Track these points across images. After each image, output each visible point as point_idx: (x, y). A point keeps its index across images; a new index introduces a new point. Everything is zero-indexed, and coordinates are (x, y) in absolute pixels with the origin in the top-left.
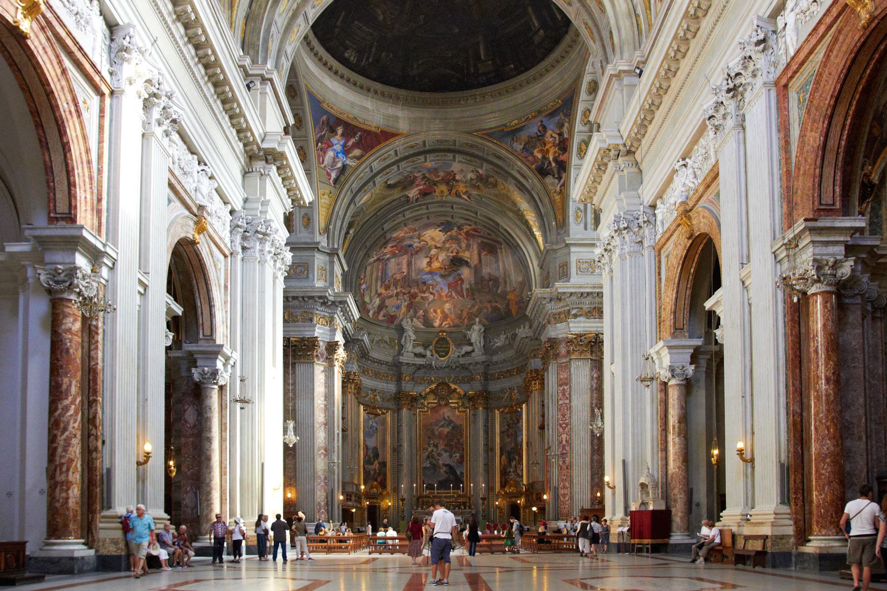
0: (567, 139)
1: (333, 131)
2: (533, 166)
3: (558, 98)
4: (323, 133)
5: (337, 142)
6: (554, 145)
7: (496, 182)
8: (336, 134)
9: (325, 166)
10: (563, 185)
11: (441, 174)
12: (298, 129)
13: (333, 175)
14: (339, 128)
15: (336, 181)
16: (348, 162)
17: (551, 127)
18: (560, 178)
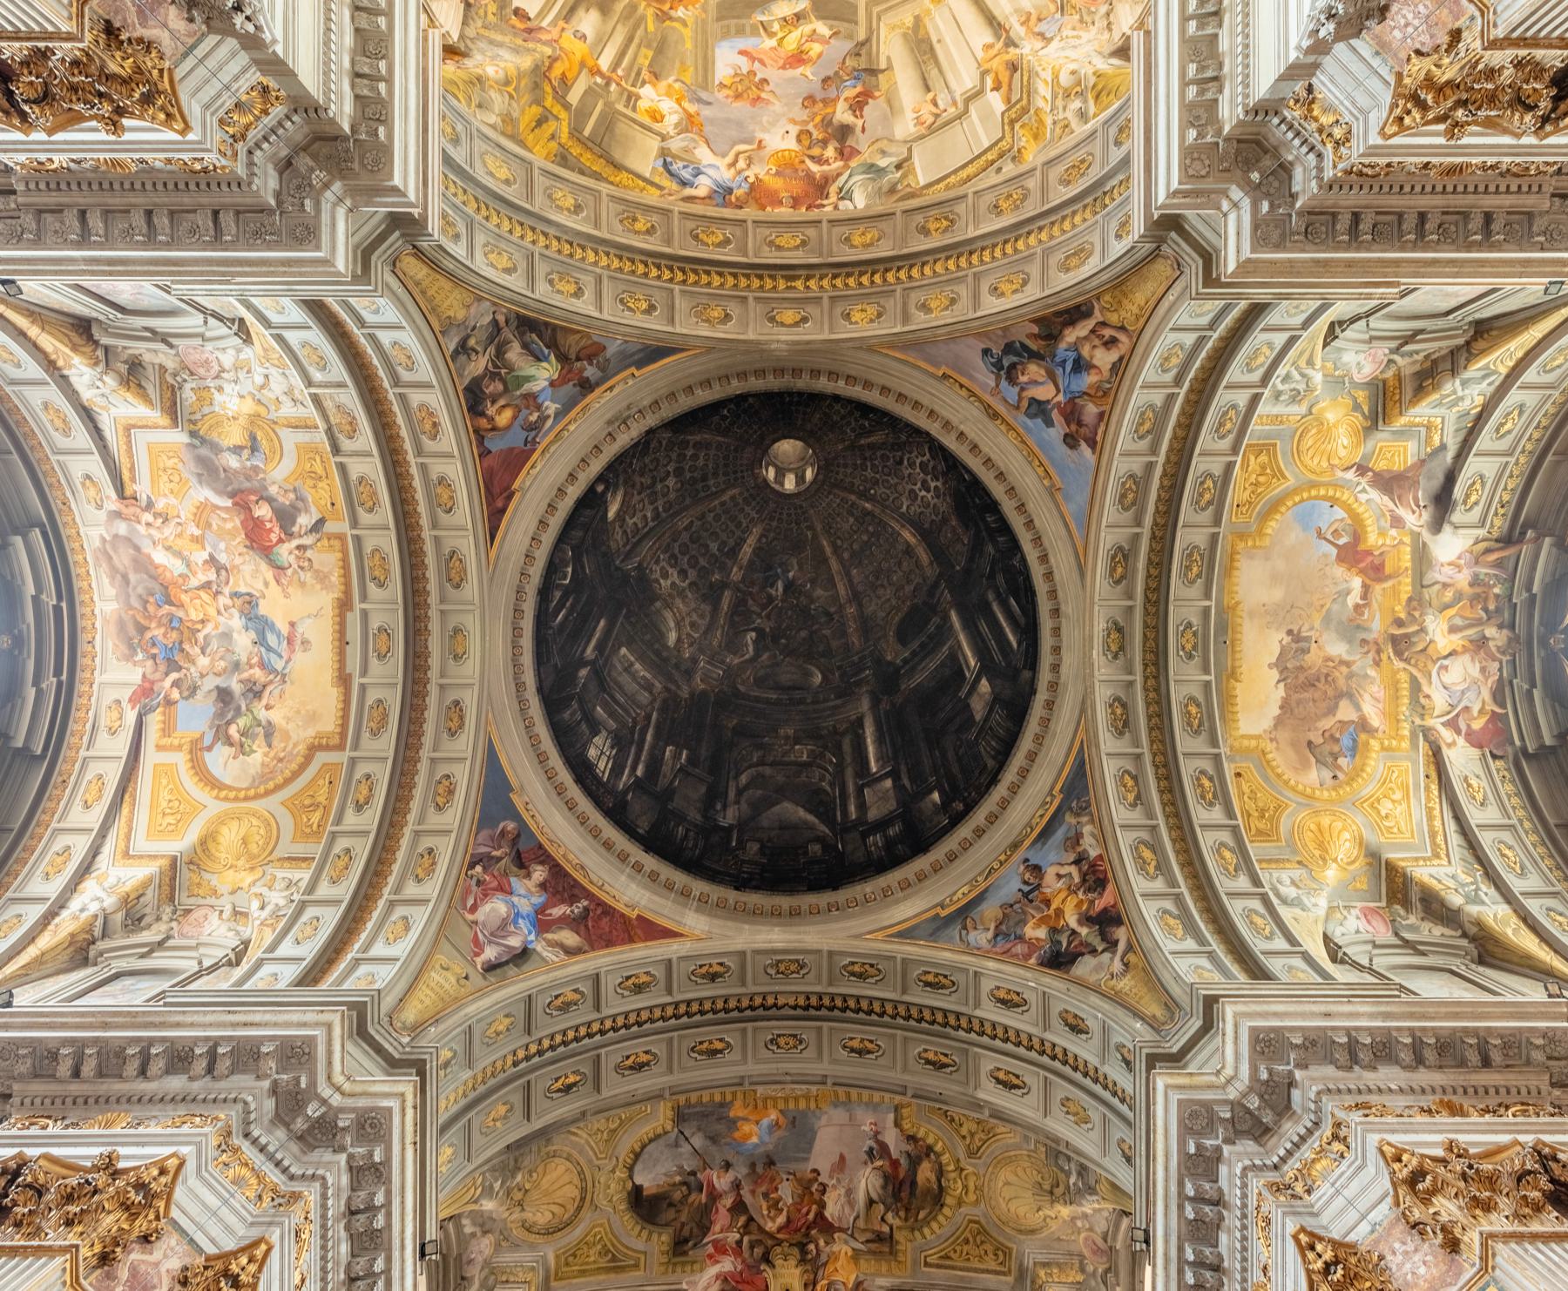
0: (1100, 857)
1: (521, 863)
2: (1033, 961)
3: (1052, 788)
4: (495, 853)
5: (526, 892)
6: (1072, 891)
7: (940, 1172)
8: (528, 876)
9: (476, 923)
10: (1130, 948)
11: (786, 1192)
12: (439, 808)
13: (490, 953)
14: (540, 868)
15: (491, 968)
16: (539, 948)
17: (1053, 857)
18: (1112, 945)
